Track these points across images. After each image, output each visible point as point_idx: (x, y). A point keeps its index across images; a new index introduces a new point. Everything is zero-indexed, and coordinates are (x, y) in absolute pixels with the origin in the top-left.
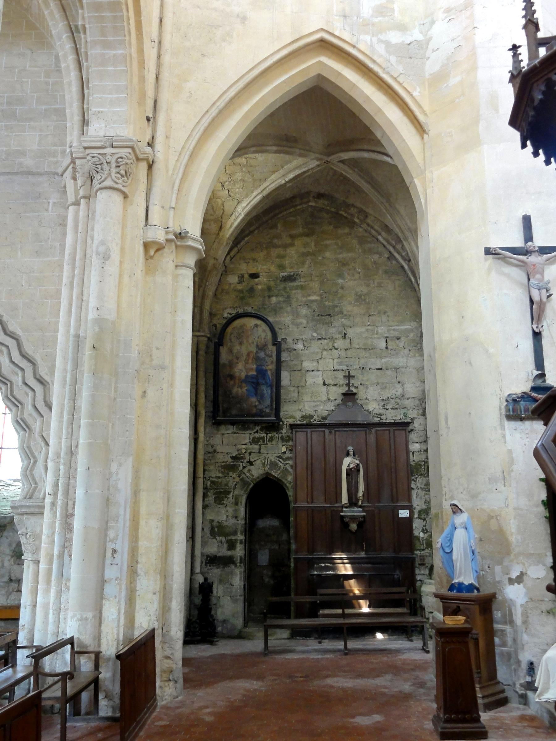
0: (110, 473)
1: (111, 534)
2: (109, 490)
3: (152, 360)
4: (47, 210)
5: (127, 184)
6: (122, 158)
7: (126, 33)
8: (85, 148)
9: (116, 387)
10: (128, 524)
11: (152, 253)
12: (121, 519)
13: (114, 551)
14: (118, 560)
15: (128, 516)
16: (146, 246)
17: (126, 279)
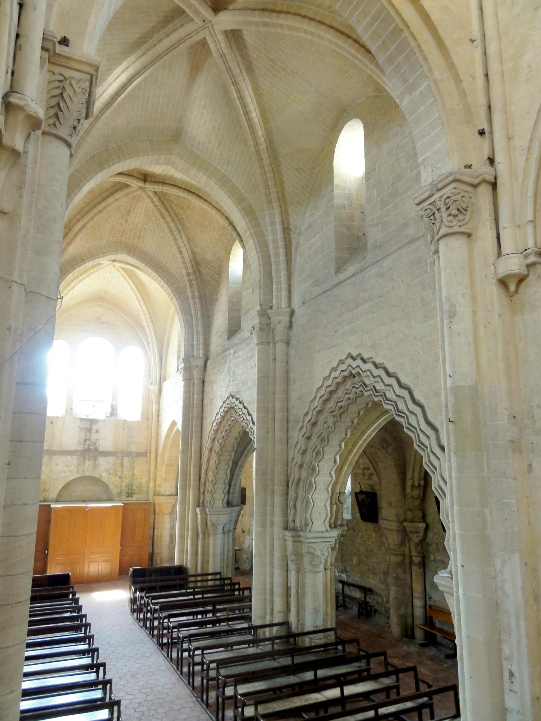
0: (495, 571)
1: (506, 651)
2: (496, 591)
3: (535, 422)
4: (426, 272)
5: (465, 222)
6: (449, 197)
7: (423, 62)
8: (418, 204)
9: (488, 464)
10: (524, 641)
11: (512, 288)
12: (514, 632)
13: (512, 674)
14: (516, 687)
15: (523, 632)
16: (503, 282)
17: (482, 331)
